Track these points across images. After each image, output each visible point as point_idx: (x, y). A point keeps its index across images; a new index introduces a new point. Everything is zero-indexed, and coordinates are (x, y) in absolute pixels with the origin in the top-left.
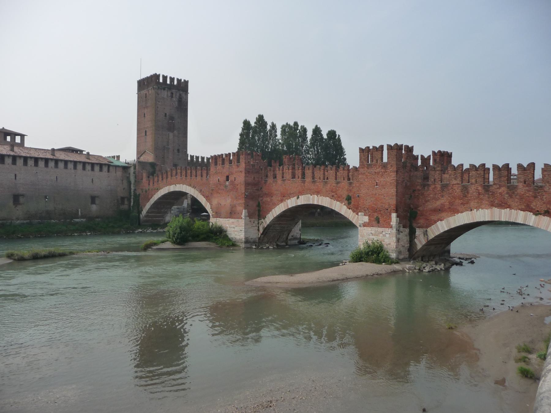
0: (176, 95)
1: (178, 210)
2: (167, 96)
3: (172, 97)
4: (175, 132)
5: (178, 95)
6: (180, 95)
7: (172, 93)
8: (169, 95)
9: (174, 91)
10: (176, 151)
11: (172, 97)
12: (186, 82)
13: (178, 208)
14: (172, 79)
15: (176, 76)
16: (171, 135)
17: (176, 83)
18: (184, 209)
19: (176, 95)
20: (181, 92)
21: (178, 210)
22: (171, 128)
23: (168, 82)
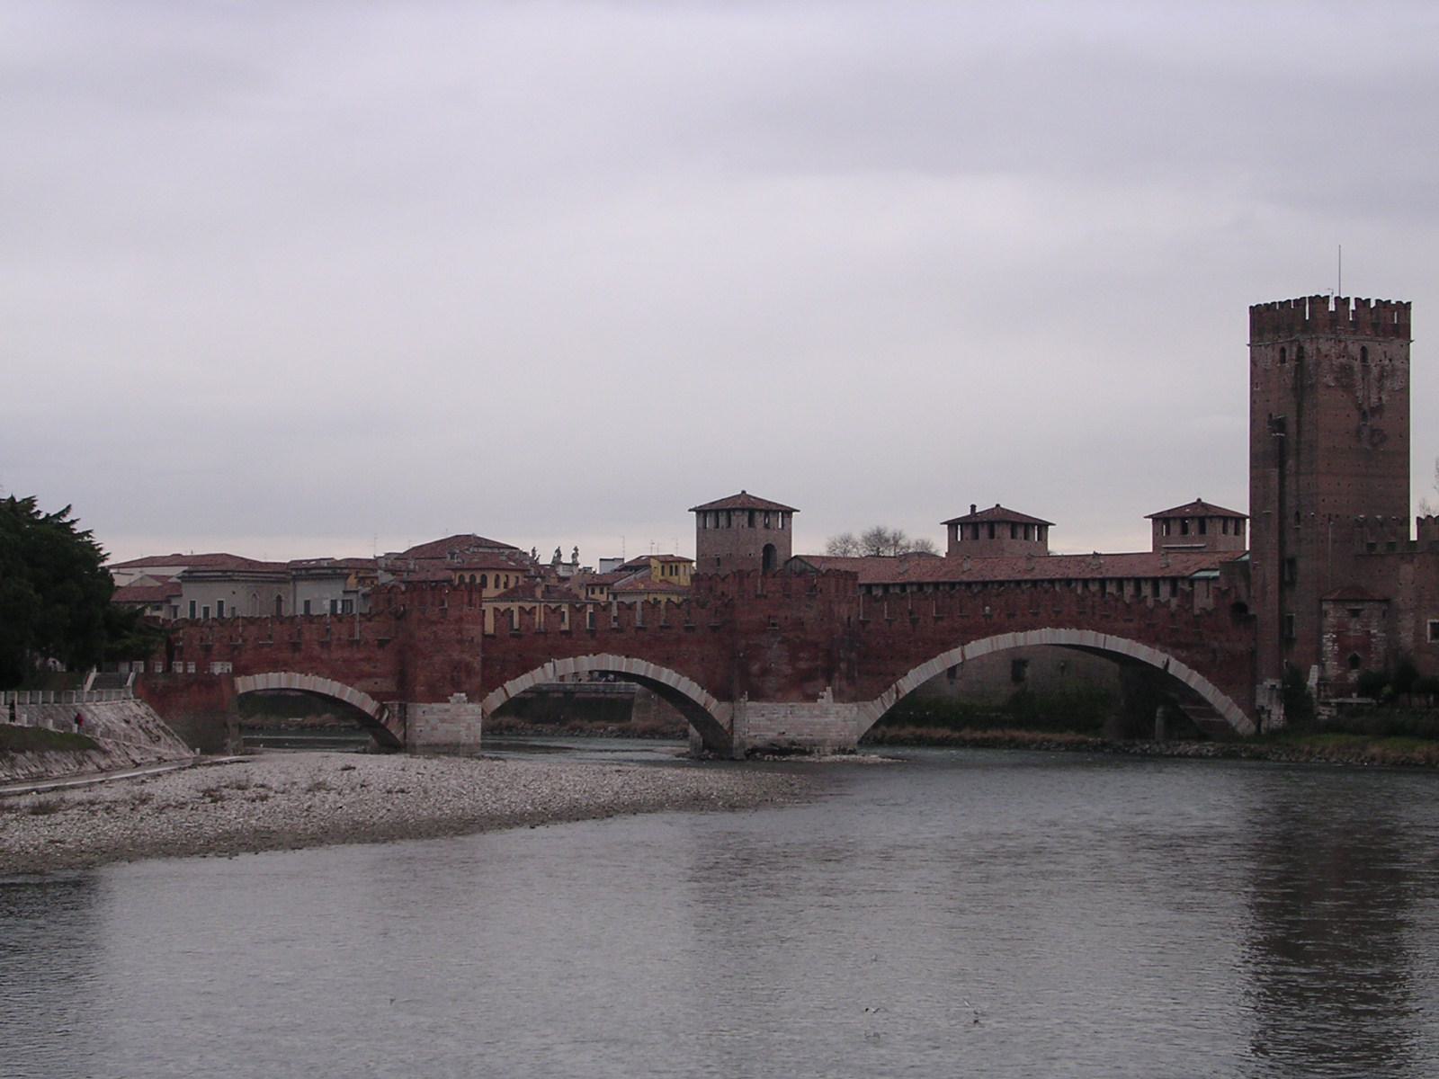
3: (1283, 360)
5: (1295, 349)
7: (1283, 350)
8: (1278, 357)
10: (1291, 520)
11: (1283, 360)
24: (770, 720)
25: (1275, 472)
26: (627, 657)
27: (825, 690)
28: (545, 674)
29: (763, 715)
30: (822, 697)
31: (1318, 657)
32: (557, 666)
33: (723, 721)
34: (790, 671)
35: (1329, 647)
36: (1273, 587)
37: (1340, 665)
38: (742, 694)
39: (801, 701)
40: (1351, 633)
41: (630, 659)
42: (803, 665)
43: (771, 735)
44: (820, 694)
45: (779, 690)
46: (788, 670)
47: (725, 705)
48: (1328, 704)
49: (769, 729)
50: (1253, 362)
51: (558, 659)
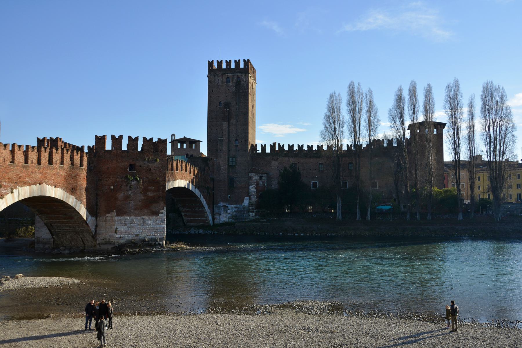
0: (233, 80)
1: (236, 209)
2: (222, 82)
3: (228, 82)
4: (232, 121)
5: (235, 78)
6: (238, 77)
8: (225, 80)
9: (230, 75)
11: (228, 82)
12: (247, 62)
13: (235, 207)
14: (228, 63)
15: (233, 59)
16: (225, 125)
17: (233, 66)
18: (244, 208)
19: (233, 80)
20: (239, 75)
21: (236, 209)
22: (227, 118)
23: (224, 66)
24: (128, 227)
25: (225, 125)
26: (55, 187)
27: (163, 209)
28: (13, 198)
29: (126, 225)
30: (162, 213)
31: (248, 194)
32: (20, 192)
33: (93, 229)
34: (143, 198)
35: (252, 189)
36: (224, 167)
37: (257, 197)
38: (109, 211)
39: (149, 215)
40: (260, 185)
41: (56, 188)
42: (150, 194)
43: (130, 237)
44: (161, 211)
45: (135, 209)
46: (141, 197)
47: (94, 218)
48: (253, 212)
49: (129, 233)
50: (210, 82)
51: (21, 187)
